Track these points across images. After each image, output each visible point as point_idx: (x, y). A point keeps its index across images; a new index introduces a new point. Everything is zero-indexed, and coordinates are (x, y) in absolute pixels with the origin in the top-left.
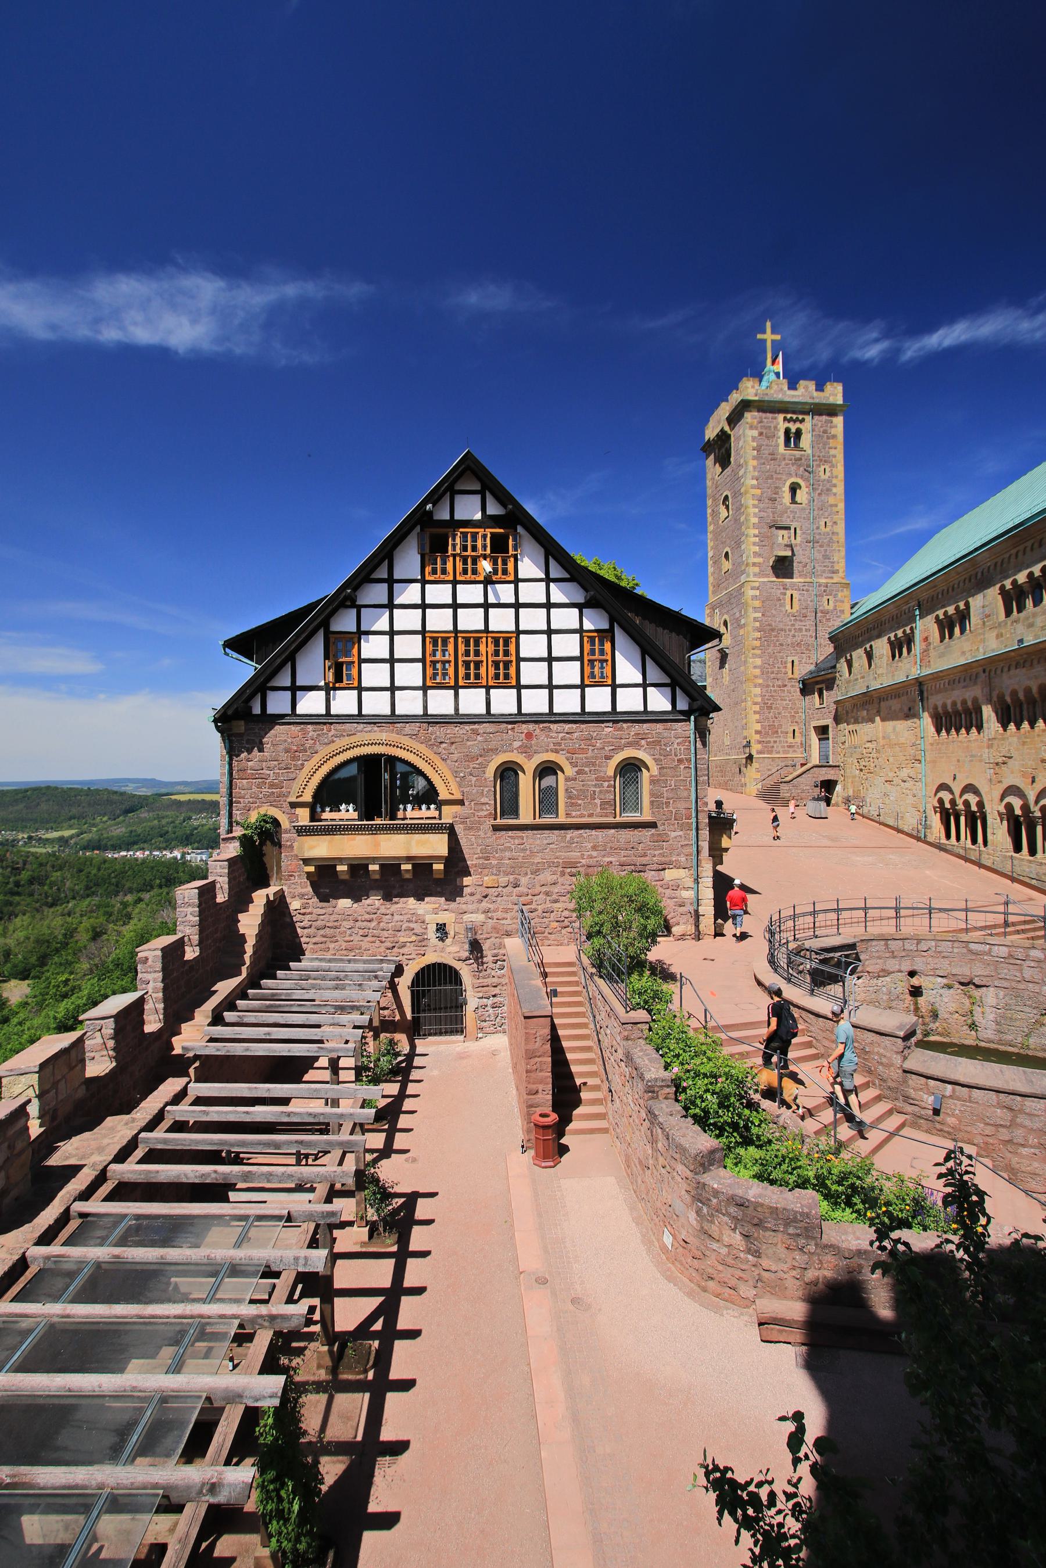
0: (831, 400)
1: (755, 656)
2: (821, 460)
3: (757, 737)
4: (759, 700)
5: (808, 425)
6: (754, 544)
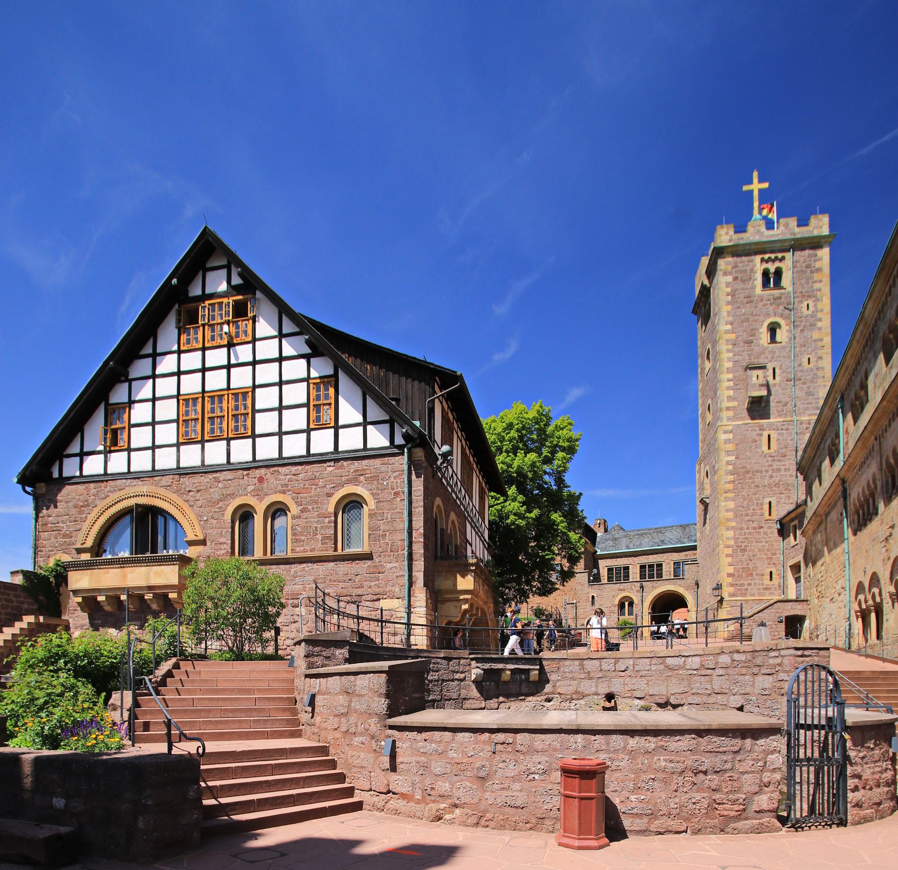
0: (816, 233)
1: (727, 499)
2: (803, 296)
3: (730, 580)
4: (732, 542)
5: (788, 264)
6: (728, 388)
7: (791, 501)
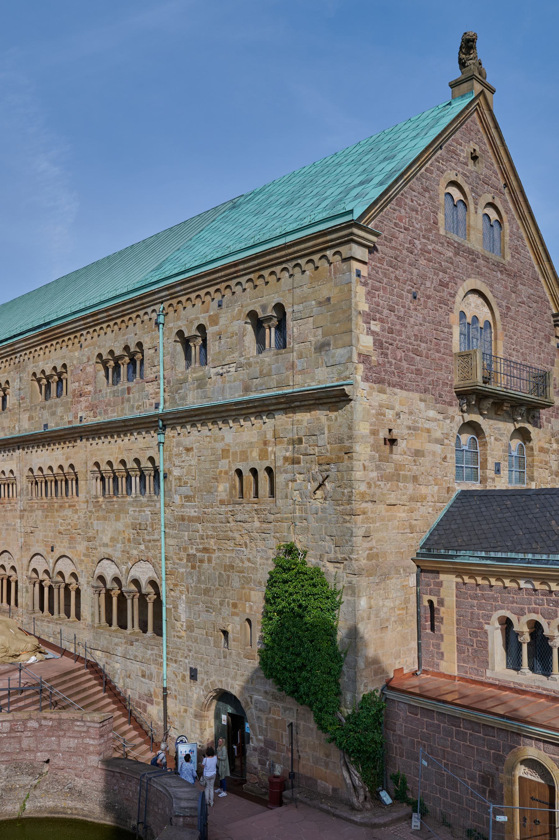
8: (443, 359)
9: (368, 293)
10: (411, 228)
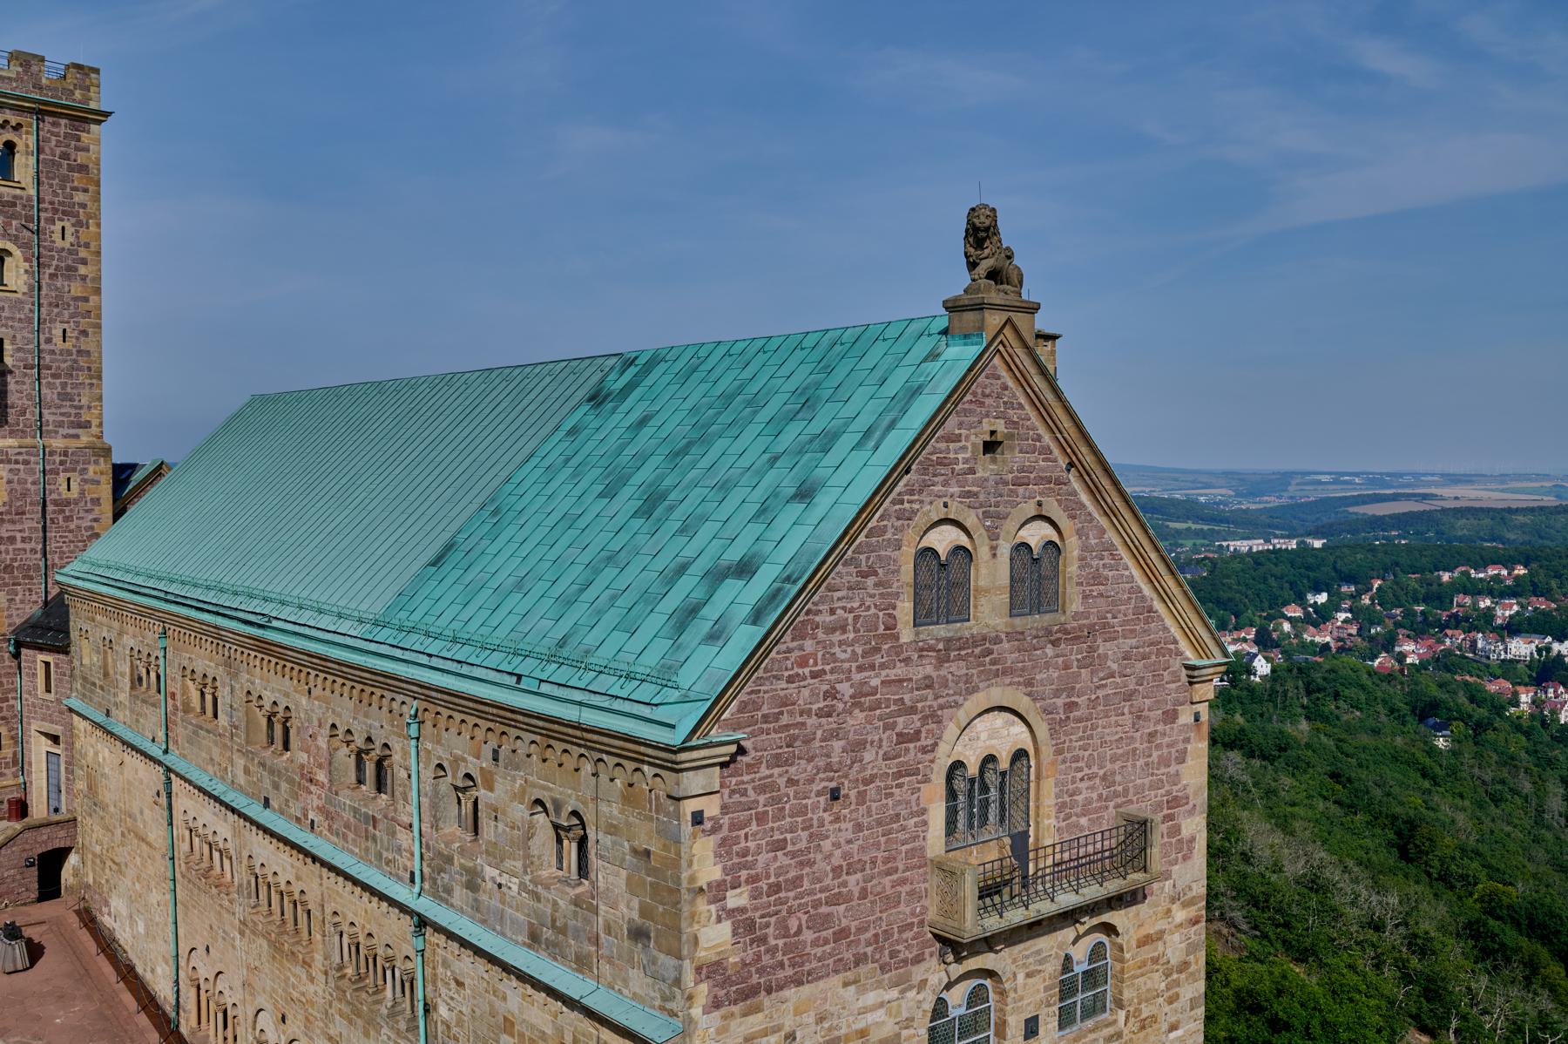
2: (55, 211)
7: (34, 597)
8: (903, 882)
9: (724, 842)
10: (827, 668)
